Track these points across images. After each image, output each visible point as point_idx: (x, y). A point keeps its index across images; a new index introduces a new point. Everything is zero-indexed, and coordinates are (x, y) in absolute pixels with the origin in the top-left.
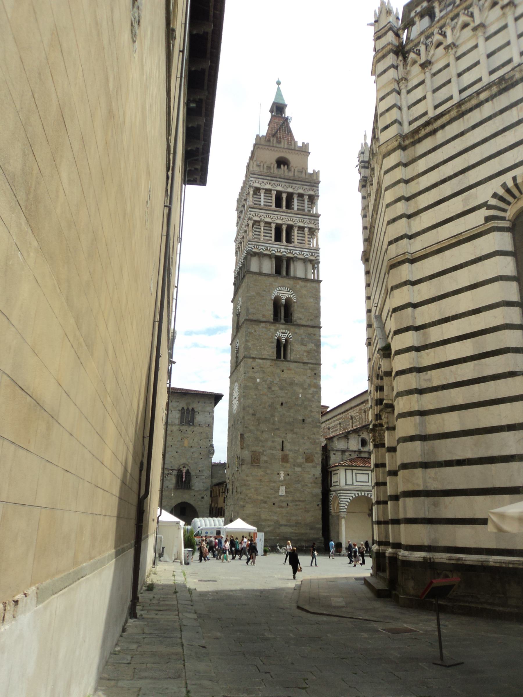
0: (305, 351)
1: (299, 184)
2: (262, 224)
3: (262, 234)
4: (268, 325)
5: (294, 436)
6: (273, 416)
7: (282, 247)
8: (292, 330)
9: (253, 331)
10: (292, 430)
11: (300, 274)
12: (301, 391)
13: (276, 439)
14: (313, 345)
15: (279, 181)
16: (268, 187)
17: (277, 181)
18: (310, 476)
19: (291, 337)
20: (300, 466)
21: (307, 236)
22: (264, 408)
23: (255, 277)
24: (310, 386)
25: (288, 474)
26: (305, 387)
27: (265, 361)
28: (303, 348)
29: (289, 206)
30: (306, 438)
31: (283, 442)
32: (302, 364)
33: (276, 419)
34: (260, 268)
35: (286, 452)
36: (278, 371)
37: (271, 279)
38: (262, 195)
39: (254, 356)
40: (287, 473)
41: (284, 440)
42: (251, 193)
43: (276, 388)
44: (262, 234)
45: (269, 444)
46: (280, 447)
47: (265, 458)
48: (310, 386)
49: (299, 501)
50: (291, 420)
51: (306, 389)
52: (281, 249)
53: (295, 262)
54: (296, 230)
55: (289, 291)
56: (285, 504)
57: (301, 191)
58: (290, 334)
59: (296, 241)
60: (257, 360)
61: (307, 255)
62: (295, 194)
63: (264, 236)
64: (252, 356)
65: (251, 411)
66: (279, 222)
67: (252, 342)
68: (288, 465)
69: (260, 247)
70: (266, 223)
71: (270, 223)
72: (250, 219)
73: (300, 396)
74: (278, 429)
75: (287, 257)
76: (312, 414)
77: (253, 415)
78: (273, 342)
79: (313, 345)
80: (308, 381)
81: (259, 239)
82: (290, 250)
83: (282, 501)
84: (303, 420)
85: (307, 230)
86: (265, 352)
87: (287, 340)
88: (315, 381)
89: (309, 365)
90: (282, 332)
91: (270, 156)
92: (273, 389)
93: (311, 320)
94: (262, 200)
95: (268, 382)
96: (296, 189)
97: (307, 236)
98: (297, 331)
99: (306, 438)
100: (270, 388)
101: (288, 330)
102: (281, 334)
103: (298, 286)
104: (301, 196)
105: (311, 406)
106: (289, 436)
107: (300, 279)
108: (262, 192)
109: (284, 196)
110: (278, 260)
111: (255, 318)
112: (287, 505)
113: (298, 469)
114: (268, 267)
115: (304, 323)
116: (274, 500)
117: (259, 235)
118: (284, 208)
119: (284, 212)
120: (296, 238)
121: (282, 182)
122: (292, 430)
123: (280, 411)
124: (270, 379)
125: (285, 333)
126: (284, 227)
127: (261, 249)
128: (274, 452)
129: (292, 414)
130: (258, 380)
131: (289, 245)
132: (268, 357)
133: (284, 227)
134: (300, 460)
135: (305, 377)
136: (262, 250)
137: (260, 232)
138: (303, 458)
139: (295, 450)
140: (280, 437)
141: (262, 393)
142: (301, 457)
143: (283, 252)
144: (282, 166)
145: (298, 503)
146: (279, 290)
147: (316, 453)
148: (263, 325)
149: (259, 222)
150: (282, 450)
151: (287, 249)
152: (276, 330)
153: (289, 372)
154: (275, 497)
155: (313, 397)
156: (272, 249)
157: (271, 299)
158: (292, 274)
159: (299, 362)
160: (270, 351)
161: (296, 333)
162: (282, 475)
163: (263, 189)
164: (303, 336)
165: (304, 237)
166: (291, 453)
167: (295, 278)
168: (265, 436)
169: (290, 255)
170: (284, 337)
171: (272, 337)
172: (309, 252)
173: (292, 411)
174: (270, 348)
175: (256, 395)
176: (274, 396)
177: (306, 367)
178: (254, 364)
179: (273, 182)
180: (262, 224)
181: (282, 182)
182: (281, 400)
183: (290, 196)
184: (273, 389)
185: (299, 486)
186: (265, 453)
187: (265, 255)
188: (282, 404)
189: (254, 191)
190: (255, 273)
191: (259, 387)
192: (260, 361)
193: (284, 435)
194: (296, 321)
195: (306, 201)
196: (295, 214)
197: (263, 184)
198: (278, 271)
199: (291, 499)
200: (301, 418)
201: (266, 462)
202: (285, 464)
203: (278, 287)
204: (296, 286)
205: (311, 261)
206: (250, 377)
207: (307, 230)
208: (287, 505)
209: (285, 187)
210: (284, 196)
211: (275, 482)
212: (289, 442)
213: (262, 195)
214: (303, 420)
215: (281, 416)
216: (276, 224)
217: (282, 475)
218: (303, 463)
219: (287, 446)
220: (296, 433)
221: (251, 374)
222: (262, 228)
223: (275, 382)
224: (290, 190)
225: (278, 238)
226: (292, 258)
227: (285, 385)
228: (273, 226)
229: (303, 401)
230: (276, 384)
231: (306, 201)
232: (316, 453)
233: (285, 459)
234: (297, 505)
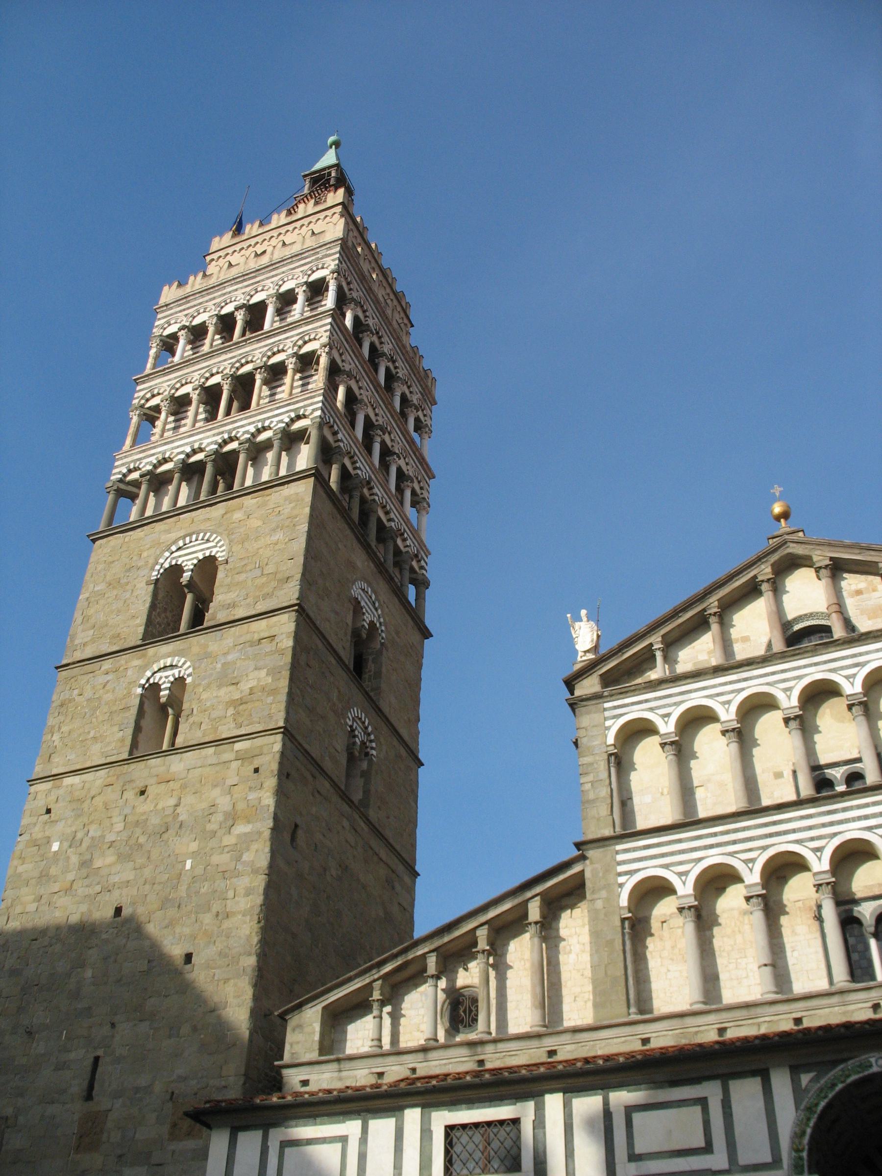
1: (283, 272)
4: (123, 659)
7: (209, 434)
13: (72, 1056)
14: (263, 673)
15: (230, 292)
19: (190, 670)
24: (232, 818)
27: (88, 777)
30: (185, 1029)
31: (97, 1059)
33: (89, 973)
35: (102, 1101)
36: (130, 795)
41: (100, 1053)
43: (104, 860)
46: (77, 1086)
48: (232, 818)
51: (214, 833)
55: (208, 541)
58: (188, 664)
60: (68, 781)
76: (226, 924)
78: (126, 708)
79: (263, 673)
80: (224, 803)
82: (230, 432)
86: (96, 748)
88: (252, 796)
89: (238, 746)
92: (98, 863)
93: (266, 596)
101: (180, 653)
102: (158, 675)
103: (238, 515)
109: (240, 317)
111: (88, 653)
115: (240, 613)
121: (236, 290)
125: (172, 666)
130: (55, 847)
135: (216, 792)
139: (137, 1090)
141: (56, 887)
143: (208, 444)
146: (179, 549)
148: (107, 665)
150: (89, 1096)
151: (222, 433)
155: (238, 859)
156: (176, 451)
166: (118, 1103)
170: (165, 679)
171: (129, 694)
172: (287, 412)
174: (116, 729)
176: (98, 888)
177: (228, 756)
181: (236, 290)
186: (21, 1119)
191: (53, 871)
193: (106, 1030)
203: (175, 542)
215: (105, 959)
227: (142, 840)
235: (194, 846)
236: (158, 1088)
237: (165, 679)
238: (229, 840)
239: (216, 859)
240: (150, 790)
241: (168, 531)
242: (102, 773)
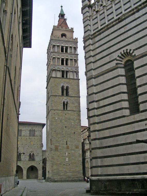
0: (74, 106)
2: (56, 59)
3: (56, 62)
4: (60, 97)
5: (71, 139)
6: (63, 132)
8: (69, 98)
9: (54, 100)
10: (70, 137)
11: (71, 77)
12: (73, 122)
13: (64, 141)
15: (62, 42)
16: (58, 44)
17: (62, 42)
18: (77, 154)
20: (73, 150)
21: (73, 62)
22: (59, 129)
23: (54, 79)
25: (69, 153)
26: (75, 120)
28: (73, 105)
29: (66, 51)
31: (67, 141)
32: (73, 112)
33: (64, 133)
34: (56, 75)
35: (68, 145)
36: (64, 114)
37: (60, 79)
38: (56, 48)
39: (55, 109)
40: (68, 153)
42: (52, 47)
43: (63, 121)
44: (56, 62)
45: (62, 142)
47: (60, 148)
49: (74, 163)
50: (70, 133)
51: (75, 121)
52: (64, 68)
53: (69, 73)
54: (69, 60)
56: (68, 165)
57: (71, 46)
59: (69, 64)
61: (74, 69)
62: (69, 47)
63: (57, 63)
64: (54, 109)
65: (54, 130)
66: (63, 57)
67: (54, 104)
68: (69, 150)
69: (56, 67)
70: (58, 58)
71: (59, 58)
72: (51, 57)
73: (73, 123)
74: (65, 137)
75: (66, 71)
76: (78, 130)
77: (55, 131)
78: (61, 104)
79: (77, 104)
81: (55, 64)
83: (67, 163)
84: (74, 133)
85: (73, 60)
86: (59, 107)
87: (67, 102)
90: (65, 99)
91: (59, 33)
92: (62, 121)
94: (56, 50)
95: (60, 119)
96: (69, 45)
97: (73, 62)
98: (71, 99)
99: (75, 139)
100: (61, 121)
104: (71, 47)
105: (77, 127)
106: (69, 139)
107: (71, 79)
108: (56, 46)
109: (64, 48)
110: (63, 72)
111: (54, 94)
112: (69, 165)
113: (73, 151)
114: (59, 75)
115: (73, 96)
116: (64, 163)
117: (55, 63)
118: (65, 52)
119: (64, 54)
120: (69, 63)
121: (63, 42)
122: (70, 137)
123: (65, 130)
124: (61, 118)
126: (65, 60)
127: (56, 68)
128: (63, 145)
129: (70, 131)
130: (56, 118)
131: (67, 66)
132: (60, 109)
133: (65, 60)
134: (74, 148)
136: (56, 69)
137: (55, 62)
138: (75, 147)
140: (65, 140)
142: (74, 147)
143: (65, 69)
144: (63, 37)
145: (73, 164)
147: (80, 145)
148: (58, 97)
149: (55, 58)
150: (67, 144)
152: (63, 99)
153: (68, 114)
154: (64, 162)
155: (78, 124)
156: (60, 68)
157: (61, 87)
158: (68, 77)
159: (72, 111)
160: (61, 107)
161: (70, 100)
162: (67, 154)
163: (56, 45)
164: (73, 101)
165: (73, 63)
167: (70, 79)
168: (60, 139)
169: (67, 70)
170: (66, 101)
171: (61, 102)
173: (70, 129)
175: (56, 124)
177: (75, 113)
178: (55, 112)
179: (60, 43)
180: (56, 59)
181: (63, 42)
182: (66, 125)
183: (67, 48)
184: (62, 121)
185: (73, 158)
187: (58, 70)
188: (66, 127)
189: (53, 46)
190: (54, 77)
192: (57, 111)
193: (67, 139)
194: (70, 95)
195: (73, 49)
196: (69, 54)
197: (56, 44)
198: (63, 76)
199: (70, 162)
200: (73, 132)
201: (60, 149)
202: (68, 150)
203: (63, 82)
204: (70, 82)
205: (75, 72)
206: (54, 117)
207: (73, 60)
208: (69, 165)
209: (65, 45)
210: (64, 48)
211: (64, 157)
212: (69, 142)
213: (56, 48)
214: (74, 133)
216: (62, 58)
217: (67, 154)
218: (75, 149)
219: (68, 143)
220: (72, 138)
221: (53, 116)
222: (56, 60)
223: (63, 119)
224: (67, 45)
225: (62, 64)
226: (68, 71)
228: (61, 59)
229: (74, 125)
230: (63, 119)
231: (73, 49)
232: (80, 145)
233: (68, 148)
234: (73, 165)
235: (73, 122)
236: (74, 144)
237: (66, 101)
238: (77, 122)
239: (75, 123)
240: (67, 114)
241: (62, 80)
242: (60, 111)
